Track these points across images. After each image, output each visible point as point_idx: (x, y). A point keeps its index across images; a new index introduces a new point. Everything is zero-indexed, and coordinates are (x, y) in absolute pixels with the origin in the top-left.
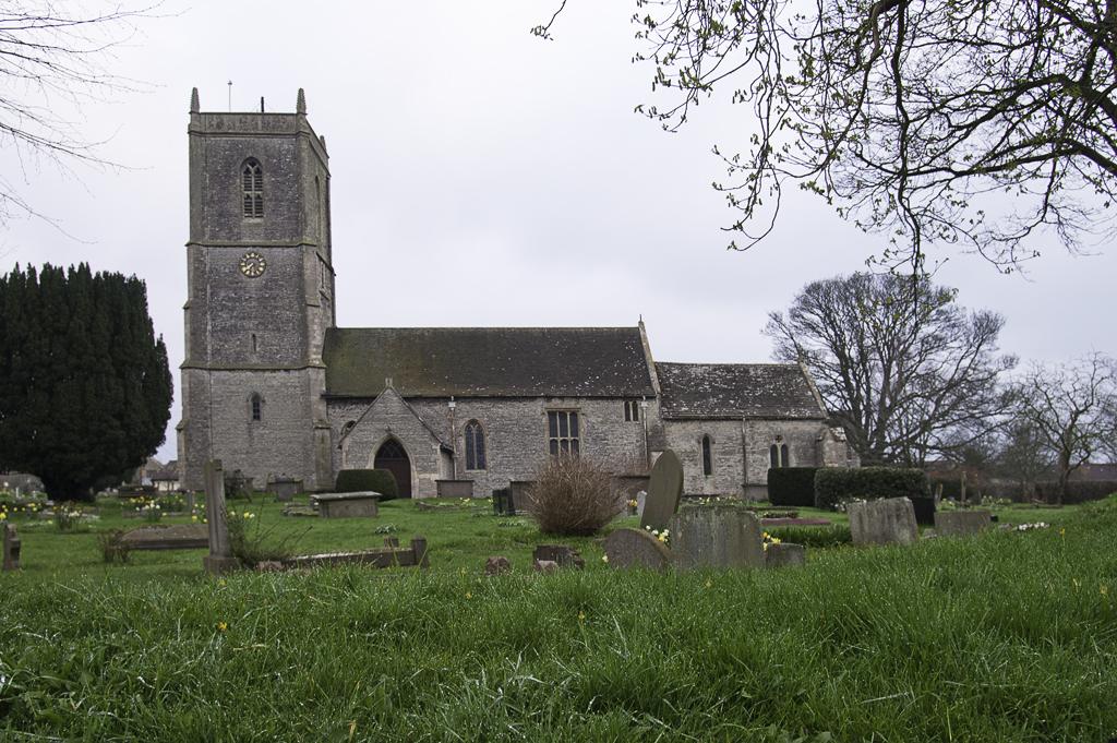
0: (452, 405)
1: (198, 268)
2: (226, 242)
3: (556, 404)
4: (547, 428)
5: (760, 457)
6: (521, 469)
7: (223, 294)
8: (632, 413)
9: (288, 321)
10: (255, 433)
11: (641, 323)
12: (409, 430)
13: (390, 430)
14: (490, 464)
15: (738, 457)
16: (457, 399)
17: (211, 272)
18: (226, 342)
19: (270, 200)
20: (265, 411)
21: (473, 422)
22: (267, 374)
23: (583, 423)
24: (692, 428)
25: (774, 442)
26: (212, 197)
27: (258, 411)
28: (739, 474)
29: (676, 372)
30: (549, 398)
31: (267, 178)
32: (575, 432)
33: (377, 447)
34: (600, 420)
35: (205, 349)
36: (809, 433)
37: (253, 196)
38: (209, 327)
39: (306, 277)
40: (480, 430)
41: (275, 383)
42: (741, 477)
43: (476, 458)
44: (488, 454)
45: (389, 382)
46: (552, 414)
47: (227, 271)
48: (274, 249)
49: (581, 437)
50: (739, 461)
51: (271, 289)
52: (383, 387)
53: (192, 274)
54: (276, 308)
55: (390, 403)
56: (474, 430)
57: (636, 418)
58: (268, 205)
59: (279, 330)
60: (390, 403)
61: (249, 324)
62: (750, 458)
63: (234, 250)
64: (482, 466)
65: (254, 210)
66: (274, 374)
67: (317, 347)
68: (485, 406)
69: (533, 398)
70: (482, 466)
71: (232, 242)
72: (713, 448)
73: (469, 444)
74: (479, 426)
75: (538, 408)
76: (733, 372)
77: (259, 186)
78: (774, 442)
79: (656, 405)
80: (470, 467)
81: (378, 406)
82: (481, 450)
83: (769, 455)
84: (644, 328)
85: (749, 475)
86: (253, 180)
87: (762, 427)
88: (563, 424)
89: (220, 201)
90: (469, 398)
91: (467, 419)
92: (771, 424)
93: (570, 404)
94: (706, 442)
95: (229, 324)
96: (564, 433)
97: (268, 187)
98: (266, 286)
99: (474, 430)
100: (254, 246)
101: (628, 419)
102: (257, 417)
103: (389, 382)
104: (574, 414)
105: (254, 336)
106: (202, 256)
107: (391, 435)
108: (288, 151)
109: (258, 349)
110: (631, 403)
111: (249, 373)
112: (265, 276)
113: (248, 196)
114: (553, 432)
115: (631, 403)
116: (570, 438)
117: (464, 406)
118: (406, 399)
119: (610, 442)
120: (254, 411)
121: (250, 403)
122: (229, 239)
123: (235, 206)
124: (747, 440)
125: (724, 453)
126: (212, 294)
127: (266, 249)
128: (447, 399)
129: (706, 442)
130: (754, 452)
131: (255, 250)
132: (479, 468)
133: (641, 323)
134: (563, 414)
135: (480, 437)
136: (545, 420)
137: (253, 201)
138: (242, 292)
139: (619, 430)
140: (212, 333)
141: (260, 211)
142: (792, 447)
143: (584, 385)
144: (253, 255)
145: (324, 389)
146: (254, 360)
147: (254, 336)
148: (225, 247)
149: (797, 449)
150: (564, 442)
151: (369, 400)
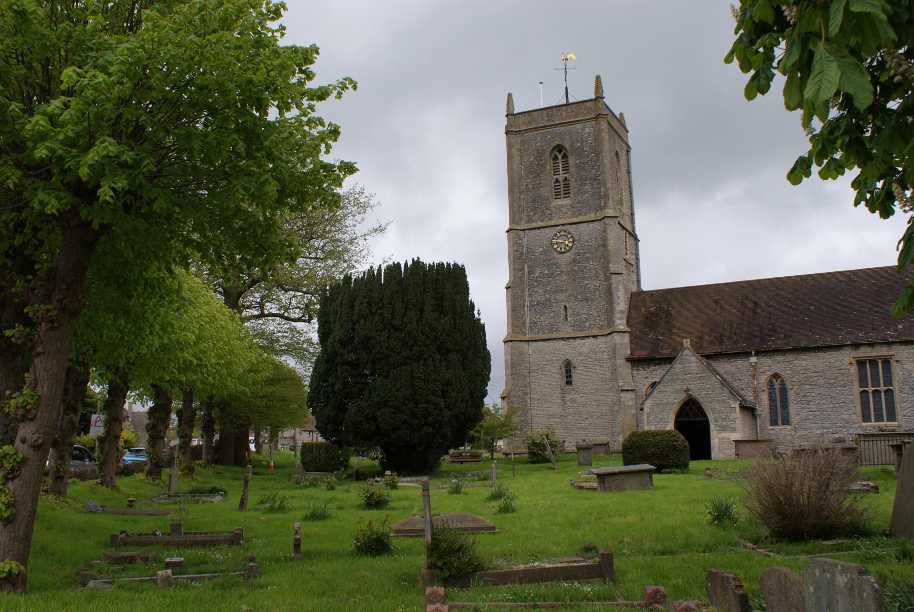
0: (753, 360)
1: (517, 251)
2: (540, 224)
3: (866, 352)
4: (856, 378)
7: (538, 271)
9: (596, 289)
14: (794, 419)
16: (757, 354)
17: (528, 253)
18: (542, 315)
19: (576, 181)
21: (776, 376)
22: (578, 342)
23: (896, 370)
26: (527, 185)
27: (570, 377)
30: (856, 346)
31: (572, 161)
32: (889, 381)
33: (675, 408)
35: (525, 322)
37: (561, 179)
38: (527, 303)
39: (609, 248)
40: (783, 384)
41: (584, 349)
44: (793, 408)
46: (861, 363)
47: (541, 250)
48: (581, 225)
49: (896, 387)
54: (584, 279)
56: (777, 385)
59: (587, 299)
61: (562, 297)
64: (786, 421)
65: (562, 193)
66: (583, 341)
67: (621, 312)
68: (787, 359)
69: (839, 347)
70: (786, 421)
73: (772, 400)
74: (782, 381)
75: (845, 359)
77: (566, 169)
80: (774, 422)
82: (785, 406)
86: (560, 164)
88: (874, 371)
89: (534, 188)
90: (770, 351)
93: (882, 351)
96: (876, 383)
98: (575, 261)
99: (777, 385)
100: (563, 225)
102: (569, 383)
103: (687, 342)
104: (887, 362)
105: (565, 307)
106: (520, 239)
107: (690, 395)
109: (569, 319)
111: (562, 342)
112: (573, 251)
113: (557, 180)
114: (863, 382)
116: (882, 388)
117: (766, 361)
118: (707, 357)
120: (567, 377)
121: (564, 370)
123: (547, 191)
126: (529, 272)
128: (747, 354)
131: (564, 228)
132: (783, 424)
134: (873, 362)
135: (784, 391)
136: (854, 369)
137: (561, 183)
140: (530, 307)
141: (567, 193)
143: (897, 329)
145: (629, 352)
146: (567, 331)
147: (565, 307)
148: (539, 228)
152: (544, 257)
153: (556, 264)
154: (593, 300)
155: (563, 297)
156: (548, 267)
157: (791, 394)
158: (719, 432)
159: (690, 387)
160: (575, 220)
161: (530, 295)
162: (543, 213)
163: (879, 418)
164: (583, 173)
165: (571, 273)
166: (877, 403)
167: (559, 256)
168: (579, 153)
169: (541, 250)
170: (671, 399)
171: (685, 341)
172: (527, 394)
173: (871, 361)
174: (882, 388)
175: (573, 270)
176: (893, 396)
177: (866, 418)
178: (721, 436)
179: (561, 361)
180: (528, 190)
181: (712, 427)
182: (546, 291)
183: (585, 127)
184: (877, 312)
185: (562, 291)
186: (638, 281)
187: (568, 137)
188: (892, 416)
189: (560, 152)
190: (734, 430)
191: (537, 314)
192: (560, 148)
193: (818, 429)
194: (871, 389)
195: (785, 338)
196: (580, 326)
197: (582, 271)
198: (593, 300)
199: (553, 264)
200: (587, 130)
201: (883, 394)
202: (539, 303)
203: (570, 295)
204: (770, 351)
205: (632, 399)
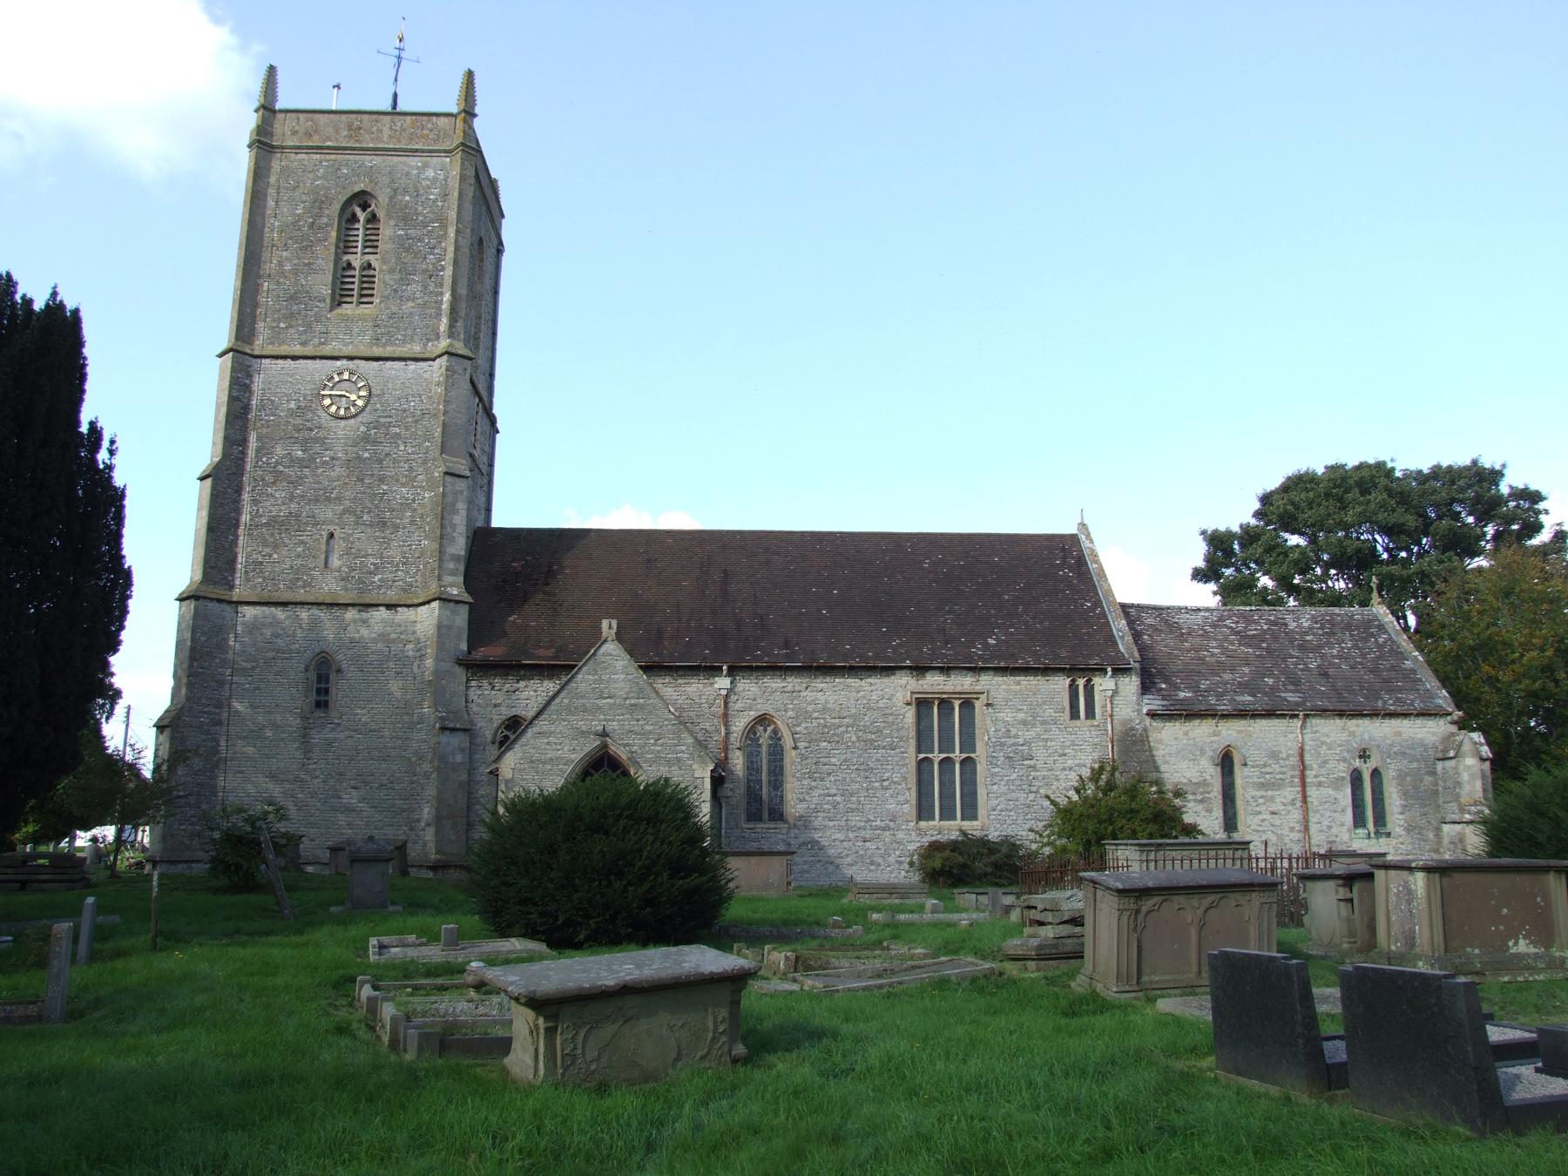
0: (723, 682)
2: (298, 349)
3: (934, 683)
4: (913, 733)
5: (1331, 792)
6: (855, 820)
7: (279, 450)
8: (1080, 707)
10: (316, 738)
11: (1083, 526)
12: (646, 734)
13: (604, 734)
15: (1291, 792)
16: (733, 671)
17: (262, 407)
18: (276, 546)
20: (340, 691)
22: (351, 614)
24: (1204, 733)
25: (1357, 763)
26: (280, 264)
27: (327, 691)
28: (1292, 829)
30: (920, 670)
31: (387, 230)
32: (969, 743)
34: (1021, 716)
36: (1422, 744)
37: (357, 263)
38: (245, 518)
42: (1296, 836)
45: (608, 627)
46: (922, 704)
47: (293, 405)
48: (389, 364)
49: (980, 753)
50: (1293, 802)
51: (375, 442)
52: (596, 639)
53: (224, 410)
54: (382, 480)
55: (612, 665)
56: (764, 738)
57: (1090, 714)
58: (384, 278)
59: (383, 524)
60: (612, 665)
61: (327, 512)
62: (1313, 793)
63: (318, 364)
66: (365, 615)
67: (455, 558)
68: (790, 688)
69: (888, 671)
71: (308, 351)
72: (1240, 776)
74: (775, 731)
75: (899, 689)
77: (371, 244)
78: (1357, 763)
79: (1131, 684)
81: (584, 679)
83: (1349, 791)
84: (1088, 536)
85: (1313, 828)
86: (361, 232)
87: (1333, 734)
89: (295, 272)
90: (759, 668)
91: (753, 714)
92: (1353, 724)
93: (961, 683)
94: (1226, 762)
95: (284, 511)
96: (946, 745)
97: (389, 246)
98: (366, 438)
99: (764, 738)
100: (351, 358)
101: (1074, 714)
102: (322, 704)
104: (968, 705)
105: (331, 535)
108: (435, 179)
109: (335, 562)
110: (1081, 682)
112: (365, 417)
114: (923, 742)
115: (1081, 682)
116: (957, 755)
117: (748, 687)
119: (1040, 765)
120: (319, 691)
121: (313, 676)
122: (304, 344)
124: (1307, 757)
125: (1262, 786)
126: (258, 450)
127: (375, 364)
128: (714, 671)
129: (1226, 762)
130: (1320, 784)
131: (351, 364)
133: (1083, 526)
134: (945, 704)
135: (777, 752)
136: (910, 715)
137: (357, 273)
138: (317, 448)
139: (1058, 738)
141: (365, 296)
142: (1389, 776)
143: (986, 646)
144: (346, 376)
145: (464, 646)
147: (331, 535)
148: (294, 358)
149: (1401, 777)
150: (946, 763)
152: (299, 421)
153: (322, 441)
154: (396, 528)
155: (330, 515)
156: (305, 444)
157: (790, 756)
160: (378, 352)
161: (255, 502)
162: (309, 326)
163: (947, 814)
164: (407, 258)
165: (354, 463)
166: (947, 785)
167: (333, 423)
168: (406, 217)
169: (293, 405)
172: (220, 723)
173: (942, 702)
174: (957, 755)
175: (359, 458)
176: (974, 772)
177: (923, 812)
179: (309, 654)
180: (282, 274)
182: (292, 498)
183: (426, 165)
184: (949, 612)
185: (328, 499)
186: (489, 510)
187: (386, 180)
188: (970, 812)
189: (365, 207)
191: (265, 543)
192: (362, 199)
193: (840, 829)
194: (936, 757)
195: (787, 645)
196: (360, 581)
197: (380, 461)
198: (396, 528)
199: (316, 440)
200: (430, 173)
201: (957, 766)
202: (273, 522)
203: (344, 512)
204: (759, 668)
205: (462, 750)
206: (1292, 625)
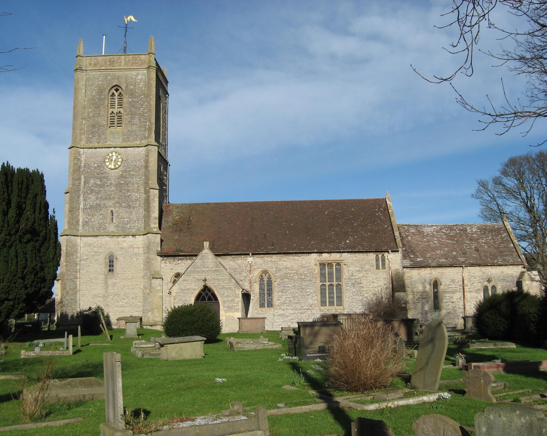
1: (76, 164)
2: (96, 145)
3: (325, 257)
4: (318, 276)
5: (476, 295)
6: (298, 306)
7: (92, 182)
8: (381, 264)
9: (137, 200)
10: (110, 282)
14: (276, 302)
17: (85, 166)
19: (128, 114)
20: (117, 266)
21: (265, 272)
22: (120, 239)
24: (428, 274)
25: (486, 283)
26: (88, 114)
29: (413, 231)
31: (126, 99)
32: (339, 278)
34: (357, 268)
35: (78, 221)
36: (512, 276)
38: (82, 206)
39: (150, 168)
40: (269, 279)
41: (125, 245)
43: (267, 300)
44: (276, 295)
46: (322, 265)
47: (96, 165)
49: (344, 283)
51: (125, 178)
54: (128, 191)
56: (266, 279)
58: (126, 118)
59: (129, 206)
61: (110, 203)
62: (467, 295)
64: (270, 305)
65: (116, 123)
66: (124, 239)
67: (155, 218)
68: (274, 260)
70: (270, 305)
71: (100, 145)
73: (261, 289)
74: (269, 276)
75: (312, 260)
76: (455, 230)
77: (120, 105)
78: (486, 283)
80: (262, 305)
82: (270, 294)
86: (116, 100)
89: (94, 117)
92: (484, 269)
93: (335, 257)
96: (331, 279)
98: (122, 176)
99: (266, 279)
101: (378, 268)
103: (206, 244)
106: (80, 155)
108: (142, 79)
109: (114, 221)
110: (380, 256)
111: (107, 238)
113: (113, 112)
115: (380, 256)
116: (335, 283)
118: (216, 255)
119: (364, 286)
120: (110, 266)
122: (98, 143)
123: (103, 121)
124: (465, 282)
126: (85, 182)
127: (124, 149)
130: (471, 291)
132: (268, 306)
134: (330, 265)
136: (317, 269)
138: (105, 180)
140: (85, 209)
141: (120, 124)
143: (346, 243)
146: (111, 228)
148: (95, 148)
150: (331, 285)
151: (196, 255)
152: (98, 171)
153: (106, 178)
154: (134, 208)
155: (111, 204)
156: (101, 179)
157: (275, 284)
158: (226, 311)
159: (208, 277)
160: (124, 144)
161: (85, 200)
162: (99, 136)
163: (331, 303)
164: (133, 110)
165: (118, 185)
166: (331, 293)
167: (110, 171)
168: (132, 94)
169: (96, 165)
170: (193, 286)
171: (205, 243)
172: (77, 278)
173: (328, 264)
174: (335, 283)
175: (120, 183)
176: (341, 289)
177: (323, 303)
178: (228, 314)
179: (106, 253)
180: (89, 117)
181: (221, 307)
182: (97, 198)
183: (138, 74)
184: (333, 231)
185: (110, 199)
187: (124, 80)
188: (340, 302)
189: (117, 90)
190: (237, 310)
191: (89, 215)
192: (117, 88)
193: (292, 309)
194: (327, 284)
195: (273, 245)
196: (122, 227)
197: (127, 184)
198: (134, 208)
199: (105, 177)
200: (140, 77)
201: (335, 287)
202: (91, 207)
203: (116, 203)
204: (262, 254)
205: (160, 285)
206: (469, 231)
